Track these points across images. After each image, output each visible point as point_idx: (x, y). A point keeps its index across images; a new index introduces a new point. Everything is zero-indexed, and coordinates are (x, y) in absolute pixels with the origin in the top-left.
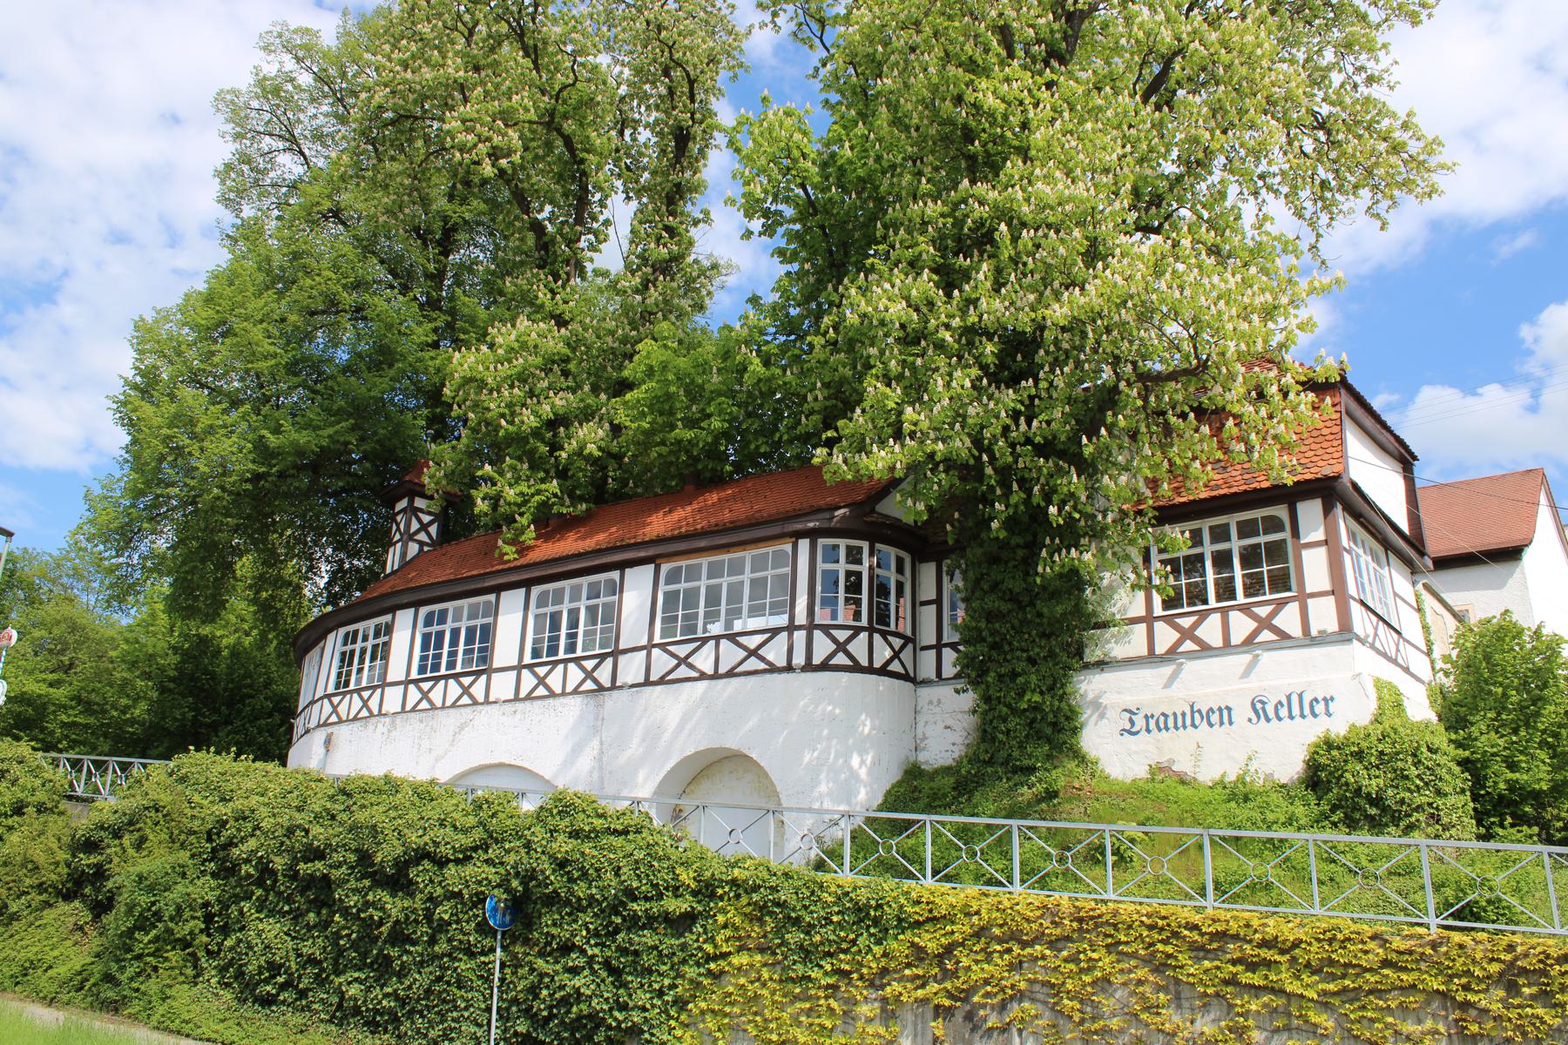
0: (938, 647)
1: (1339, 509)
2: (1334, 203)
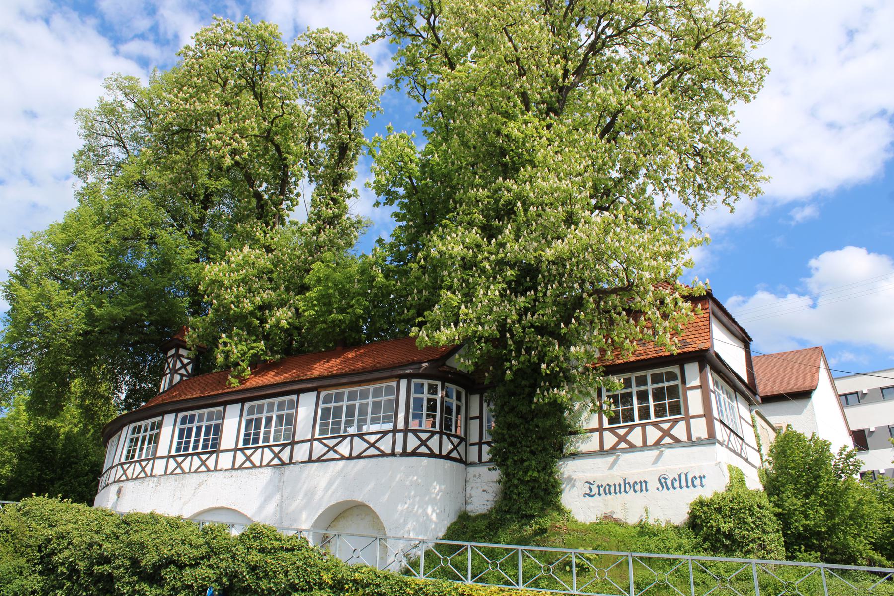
0: (480, 444)
1: (708, 368)
2: (705, 197)
